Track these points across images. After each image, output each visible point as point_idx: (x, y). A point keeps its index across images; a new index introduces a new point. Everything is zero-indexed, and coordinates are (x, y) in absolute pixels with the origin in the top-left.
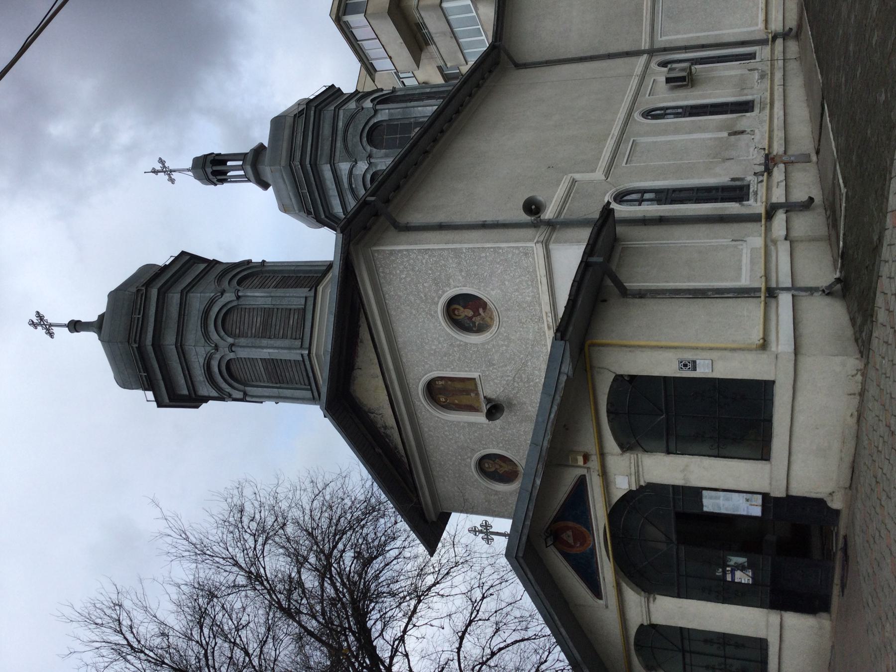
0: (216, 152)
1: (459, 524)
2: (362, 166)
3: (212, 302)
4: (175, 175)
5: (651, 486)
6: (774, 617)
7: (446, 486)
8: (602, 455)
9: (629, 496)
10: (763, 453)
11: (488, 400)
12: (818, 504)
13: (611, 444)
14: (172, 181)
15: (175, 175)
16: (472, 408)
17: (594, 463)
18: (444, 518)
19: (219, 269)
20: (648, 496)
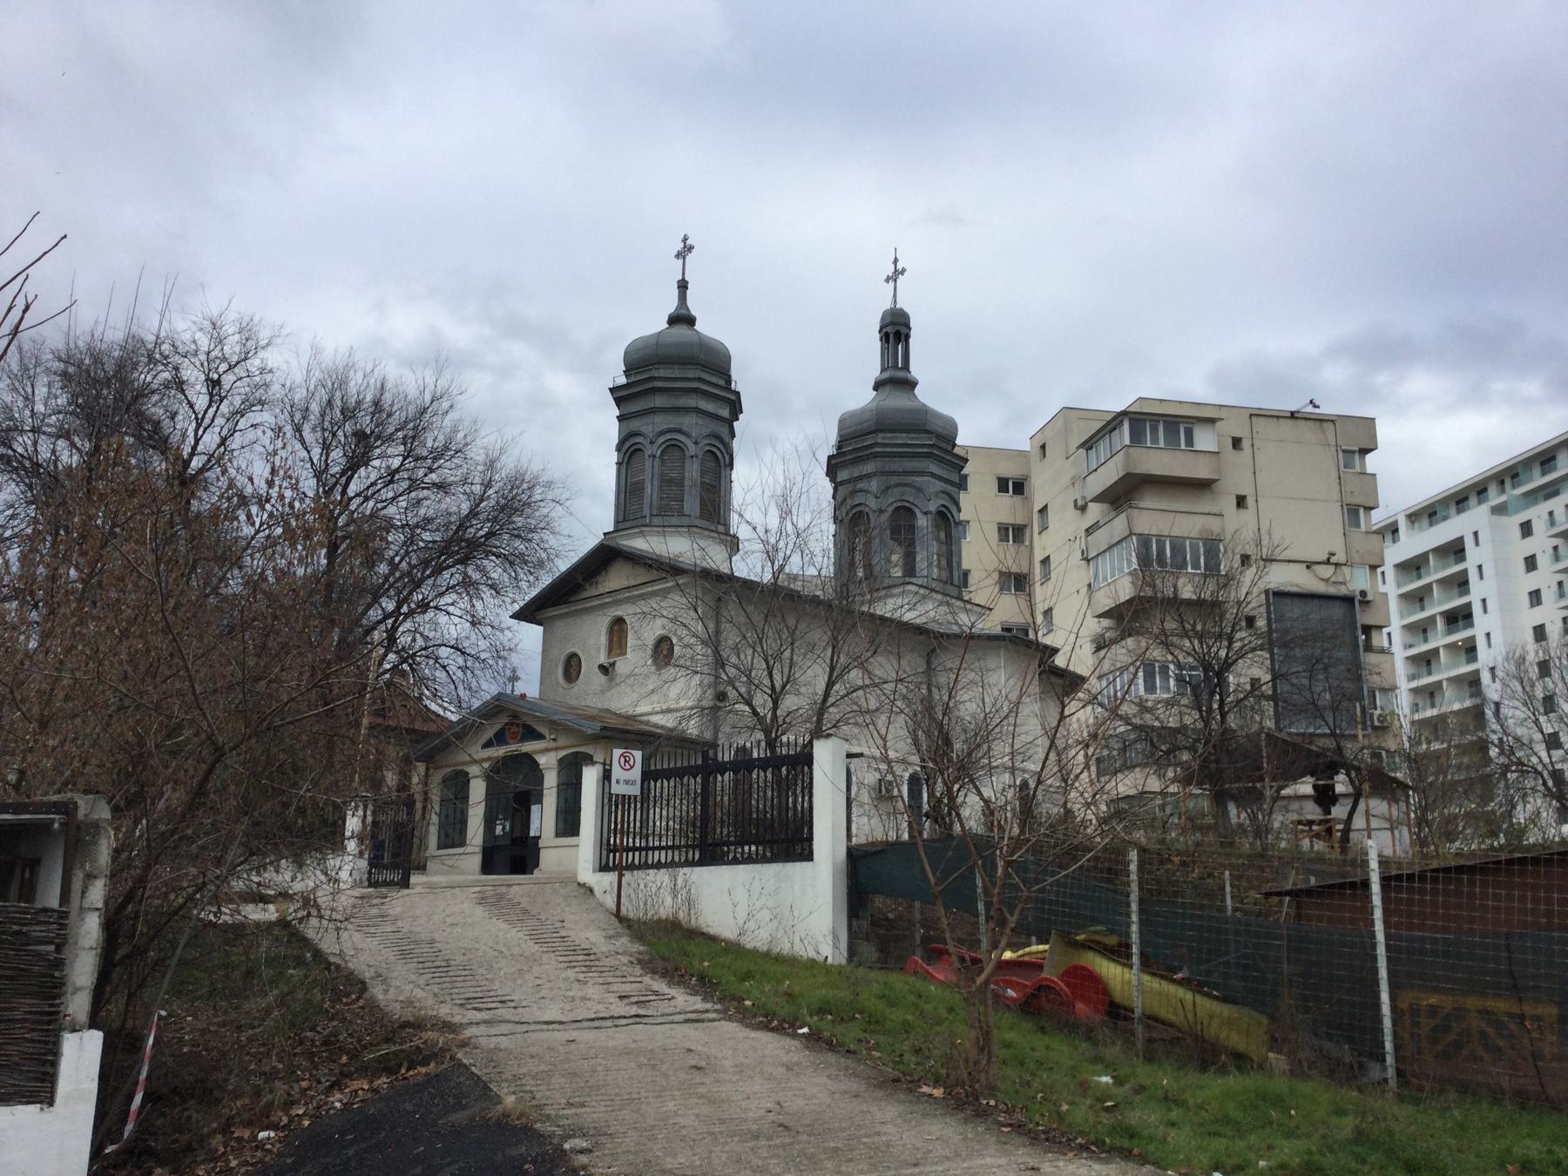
0: (912, 333)
1: (536, 632)
2: (872, 503)
3: (688, 435)
4: (891, 284)
5: (542, 777)
6: (477, 849)
7: (561, 627)
8: (556, 749)
9: (536, 764)
10: (558, 835)
11: (613, 665)
12: (537, 865)
13: (562, 754)
14: (887, 280)
15: (891, 284)
16: (610, 651)
17: (552, 744)
18: (539, 623)
19: (724, 431)
20: (536, 773)
